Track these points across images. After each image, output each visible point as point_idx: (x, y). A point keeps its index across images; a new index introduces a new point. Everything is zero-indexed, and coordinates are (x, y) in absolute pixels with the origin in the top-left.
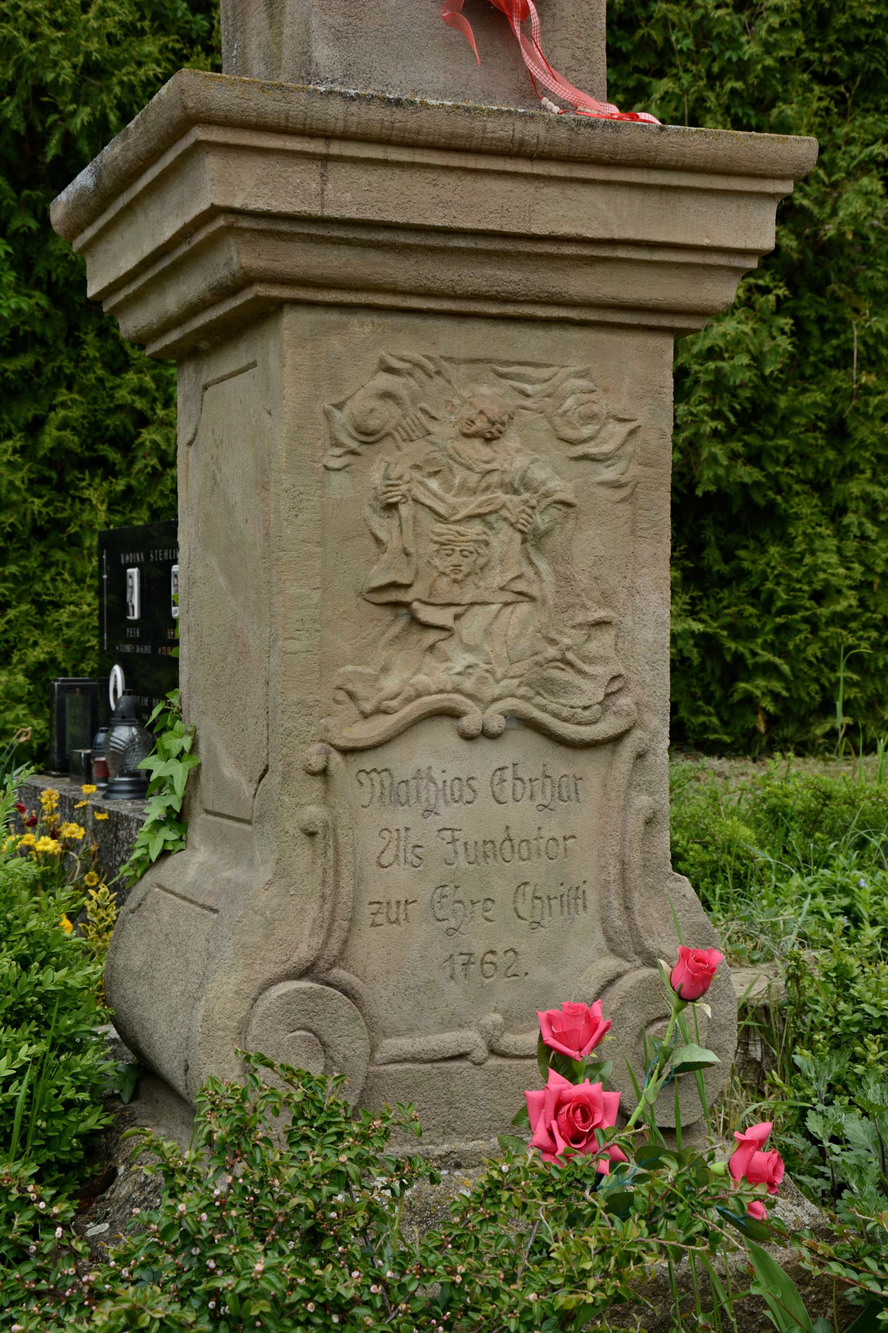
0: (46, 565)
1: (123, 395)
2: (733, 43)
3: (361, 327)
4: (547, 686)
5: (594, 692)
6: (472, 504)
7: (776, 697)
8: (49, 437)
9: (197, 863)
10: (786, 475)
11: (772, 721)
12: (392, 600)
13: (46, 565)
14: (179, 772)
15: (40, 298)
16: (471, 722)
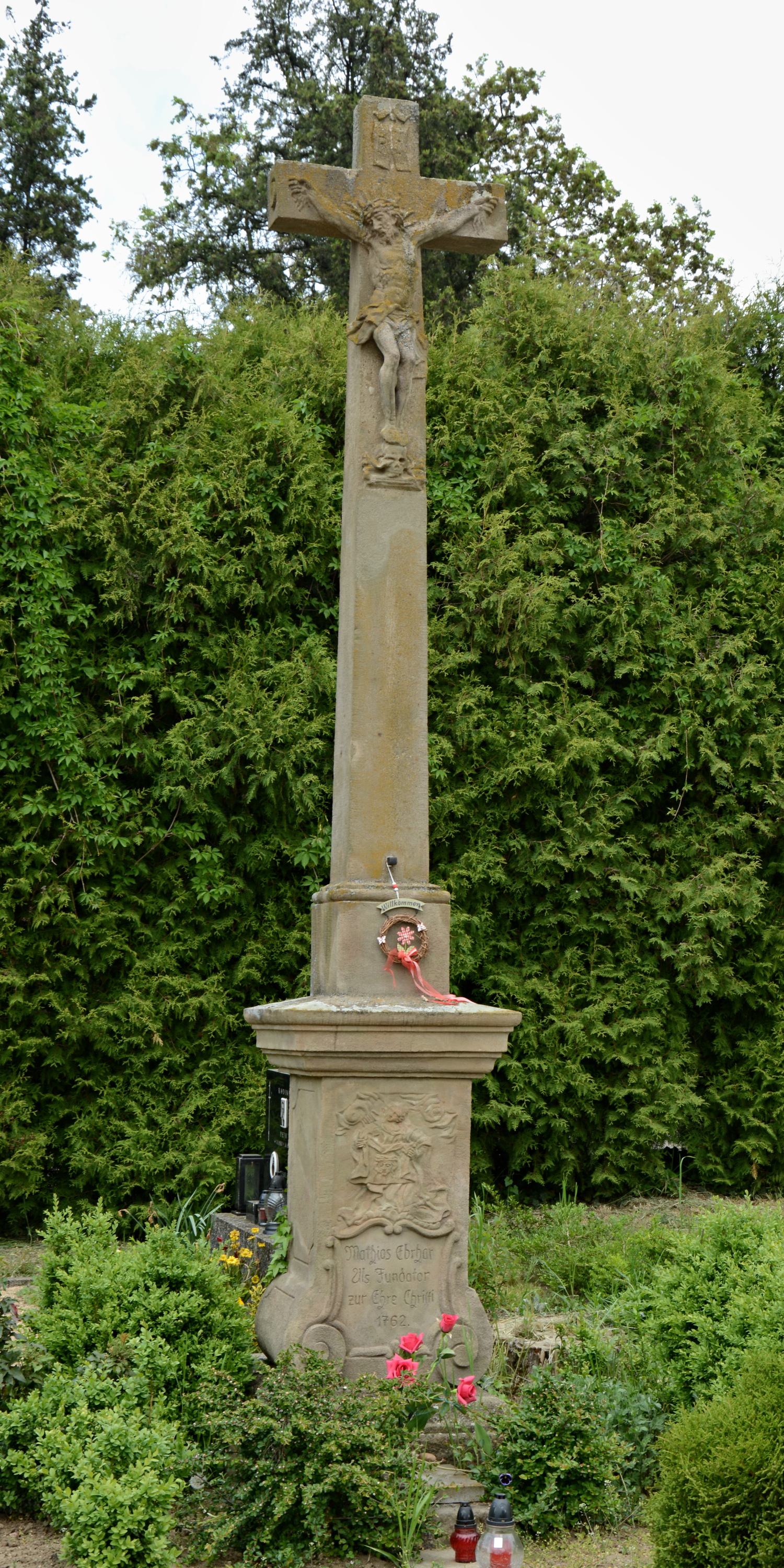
0: (236, 1057)
1: (291, 945)
2: (720, 693)
3: (350, 1084)
4: (418, 1215)
5: (437, 1217)
6: (390, 1147)
7: (766, 1153)
8: (241, 973)
9: (290, 1279)
10: (773, 986)
11: (763, 1170)
12: (360, 1183)
13: (236, 1057)
14: (285, 1241)
15: (240, 883)
16: (389, 1228)
